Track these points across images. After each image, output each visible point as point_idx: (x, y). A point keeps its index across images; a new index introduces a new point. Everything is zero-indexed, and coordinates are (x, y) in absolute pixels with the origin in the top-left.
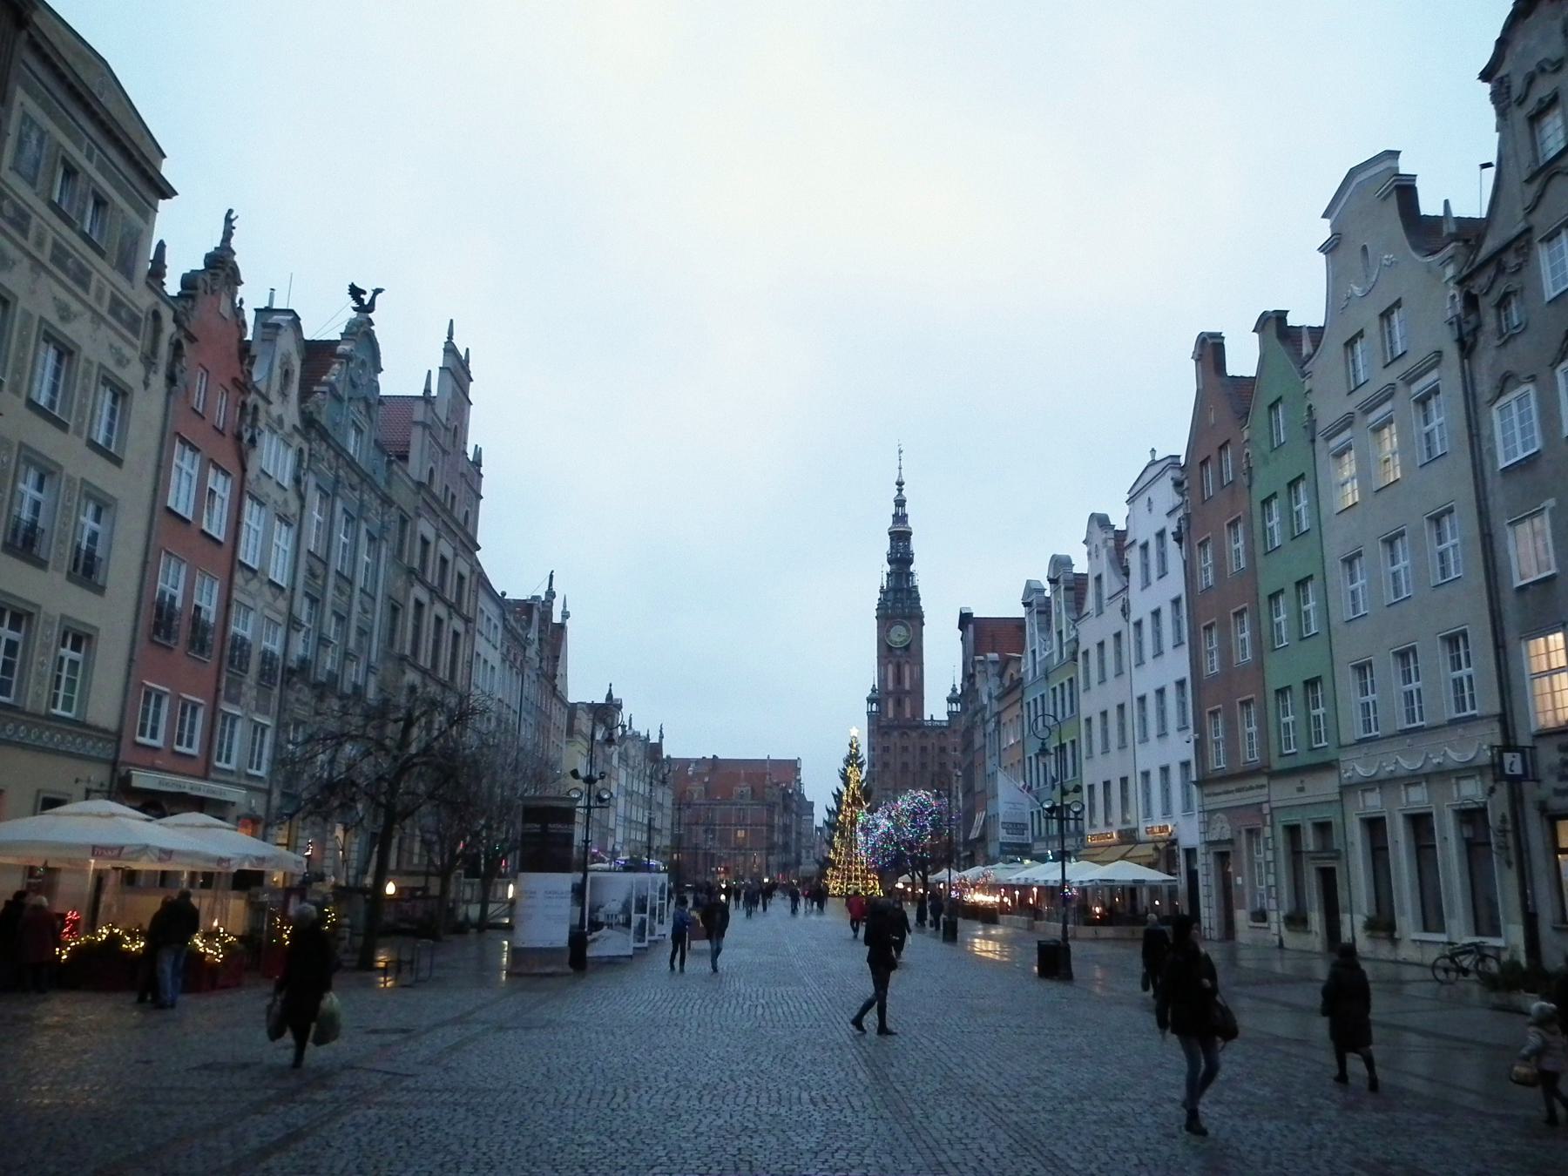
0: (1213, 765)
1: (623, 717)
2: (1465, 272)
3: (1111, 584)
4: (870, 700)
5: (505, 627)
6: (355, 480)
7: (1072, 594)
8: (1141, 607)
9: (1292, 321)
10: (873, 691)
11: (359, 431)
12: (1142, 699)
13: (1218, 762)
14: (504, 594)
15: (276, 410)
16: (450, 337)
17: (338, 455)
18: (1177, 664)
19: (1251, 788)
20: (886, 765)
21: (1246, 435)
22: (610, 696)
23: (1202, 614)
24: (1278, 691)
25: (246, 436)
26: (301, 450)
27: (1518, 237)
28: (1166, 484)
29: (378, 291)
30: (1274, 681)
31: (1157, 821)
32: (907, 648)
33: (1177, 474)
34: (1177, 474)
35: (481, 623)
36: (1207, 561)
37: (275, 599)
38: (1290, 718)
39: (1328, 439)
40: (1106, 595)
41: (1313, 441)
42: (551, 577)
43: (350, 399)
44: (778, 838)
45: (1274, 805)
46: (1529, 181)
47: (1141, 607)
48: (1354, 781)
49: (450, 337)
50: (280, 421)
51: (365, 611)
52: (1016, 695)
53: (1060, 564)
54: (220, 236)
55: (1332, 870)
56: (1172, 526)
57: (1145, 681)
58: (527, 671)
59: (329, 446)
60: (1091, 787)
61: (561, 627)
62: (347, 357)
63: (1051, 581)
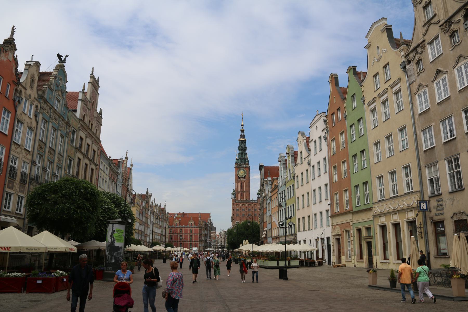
0: (336, 211)
1: (152, 199)
2: (407, 53)
3: (305, 154)
4: (233, 194)
5: (110, 168)
6: (57, 117)
7: (293, 157)
8: (314, 160)
9: (358, 70)
10: (234, 191)
11: (59, 101)
15: (29, 92)
16: (92, 73)
17: (51, 108)
18: (325, 179)
22: (147, 193)
25: (17, 100)
26: (37, 106)
27: (421, 43)
29: (67, 56)
30: (354, 183)
32: (244, 177)
33: (325, 118)
34: (325, 118)
35: (102, 167)
36: (333, 145)
37: (27, 155)
39: (369, 106)
40: (304, 157)
42: (127, 153)
44: (203, 238)
45: (354, 222)
46: (424, 26)
49: (92, 73)
50: (30, 96)
52: (277, 190)
54: (10, 34)
55: (371, 242)
56: (323, 134)
57: (315, 185)
58: (118, 183)
59: (47, 105)
60: (299, 219)
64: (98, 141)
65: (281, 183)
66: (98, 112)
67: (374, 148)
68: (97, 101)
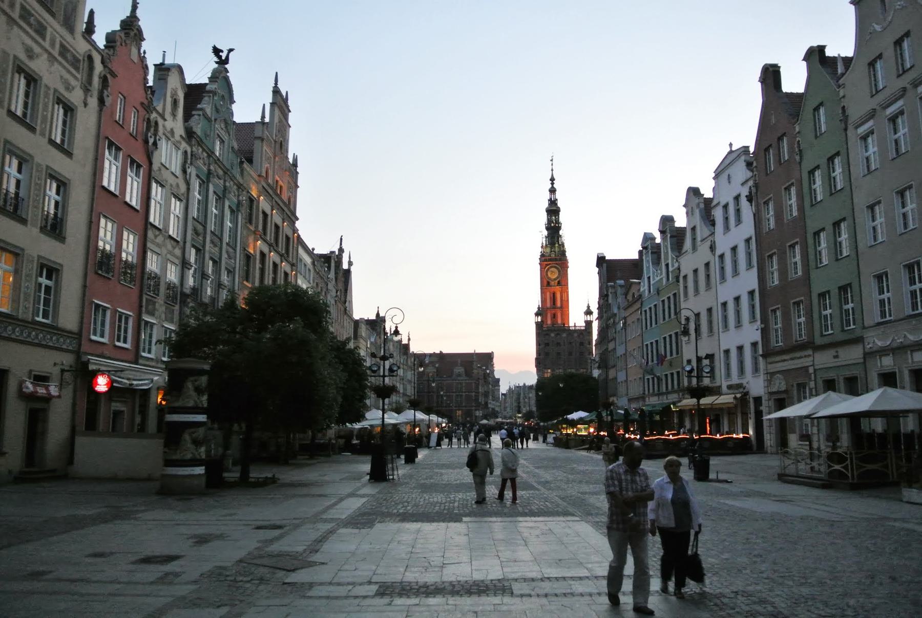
4: (537, 314)
6: (221, 172)
8: (724, 244)
9: (829, 53)
11: (222, 142)
12: (724, 304)
13: (777, 342)
14: (313, 249)
15: (169, 124)
17: (209, 156)
18: (749, 280)
19: (801, 357)
20: (547, 354)
21: (797, 130)
22: (378, 315)
23: (766, 247)
24: (819, 295)
25: (151, 141)
26: (186, 152)
28: (741, 164)
29: (230, 50)
30: (817, 289)
31: (735, 380)
37: (174, 248)
38: (829, 312)
39: (857, 128)
40: (699, 239)
41: (846, 130)
43: (215, 120)
45: (817, 367)
47: (724, 244)
48: (875, 349)
50: (172, 132)
51: (229, 257)
52: (638, 305)
53: (667, 222)
56: (745, 192)
57: (726, 292)
59: (204, 150)
61: (348, 273)
62: (214, 93)
63: (662, 232)
64: (293, 218)
65: (647, 292)
66: (291, 161)
67: (867, 214)
68: (288, 141)
